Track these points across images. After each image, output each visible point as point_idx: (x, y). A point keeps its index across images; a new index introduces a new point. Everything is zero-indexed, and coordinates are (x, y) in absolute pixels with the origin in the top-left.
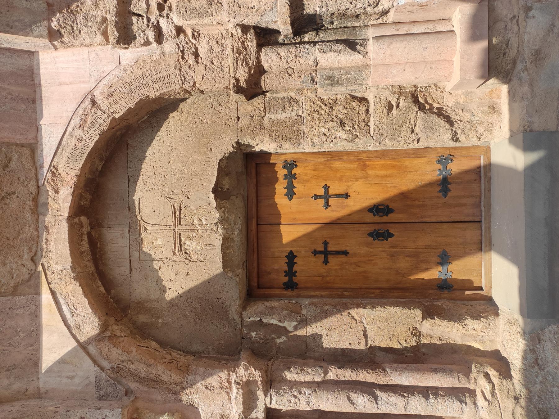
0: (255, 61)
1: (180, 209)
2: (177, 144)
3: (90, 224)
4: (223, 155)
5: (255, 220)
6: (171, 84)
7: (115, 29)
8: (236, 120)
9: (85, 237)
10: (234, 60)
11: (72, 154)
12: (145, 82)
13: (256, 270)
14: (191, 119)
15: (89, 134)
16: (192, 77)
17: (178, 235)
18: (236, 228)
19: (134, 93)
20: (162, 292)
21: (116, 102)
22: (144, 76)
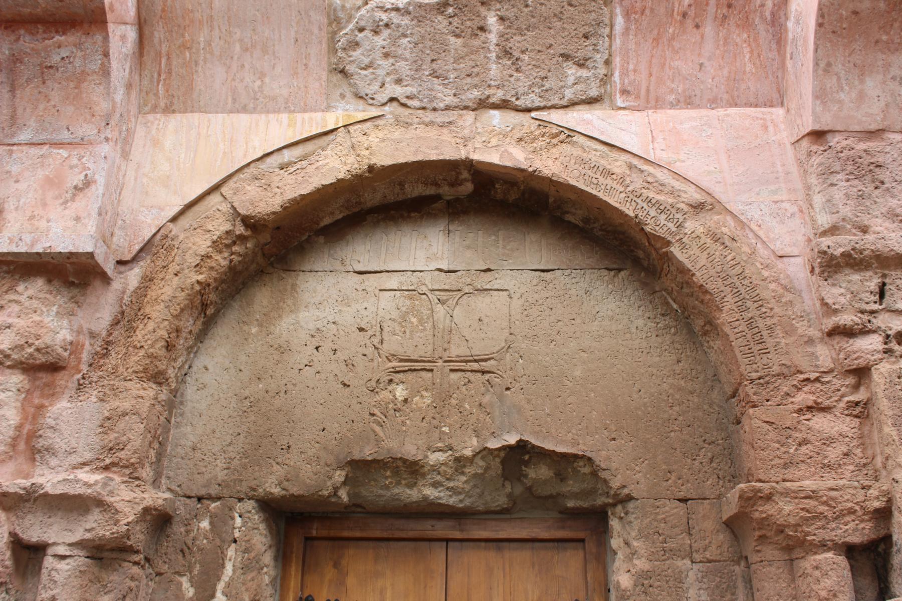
0: (814, 540)
1: (484, 372)
2: (622, 368)
3: (457, 200)
4: (603, 466)
5: (458, 535)
6: (749, 355)
7: (848, 248)
8: (681, 495)
9: (431, 191)
10: (813, 492)
11: (596, 168)
12: (749, 304)
13: (346, 534)
14: (677, 397)
15: (635, 199)
16: (768, 401)
17: (428, 366)
18: (439, 492)
19: (724, 282)
20: (312, 333)
21: (703, 248)
22: (760, 302)
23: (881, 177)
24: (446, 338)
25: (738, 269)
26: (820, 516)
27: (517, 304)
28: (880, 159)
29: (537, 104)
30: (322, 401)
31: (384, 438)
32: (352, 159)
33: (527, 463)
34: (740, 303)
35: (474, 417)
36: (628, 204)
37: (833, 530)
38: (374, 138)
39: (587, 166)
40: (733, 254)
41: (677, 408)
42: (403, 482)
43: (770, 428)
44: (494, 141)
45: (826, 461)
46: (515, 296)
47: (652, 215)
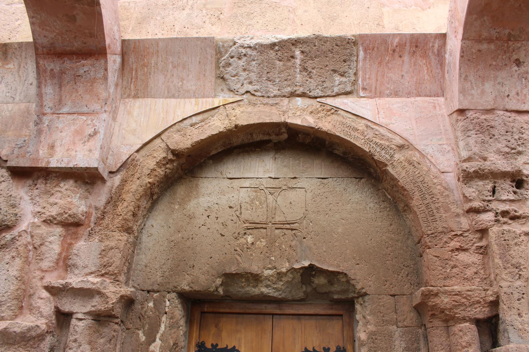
0: (459, 316)
1: (292, 230)
2: (362, 228)
3: (279, 142)
4: (352, 277)
5: (278, 312)
7: (477, 168)
8: (392, 293)
9: (266, 138)
10: (459, 292)
11: (349, 127)
12: (427, 196)
13: (222, 310)
14: (390, 243)
15: (369, 142)
16: (436, 245)
17: (264, 226)
18: (269, 290)
20: (206, 209)
21: (403, 168)
22: (432, 195)
23: (493, 133)
24: (273, 212)
25: (421, 179)
26: (462, 304)
27: (309, 195)
28: (493, 123)
29: (320, 94)
30: (210, 243)
32: (227, 122)
33: (314, 276)
34: (422, 196)
35: (287, 252)
36: (366, 145)
37: (469, 311)
38: (238, 111)
39: (345, 126)
40: (419, 171)
41: (390, 249)
42: (251, 285)
43: (437, 259)
44: (298, 113)
45: (466, 276)
46: (309, 191)
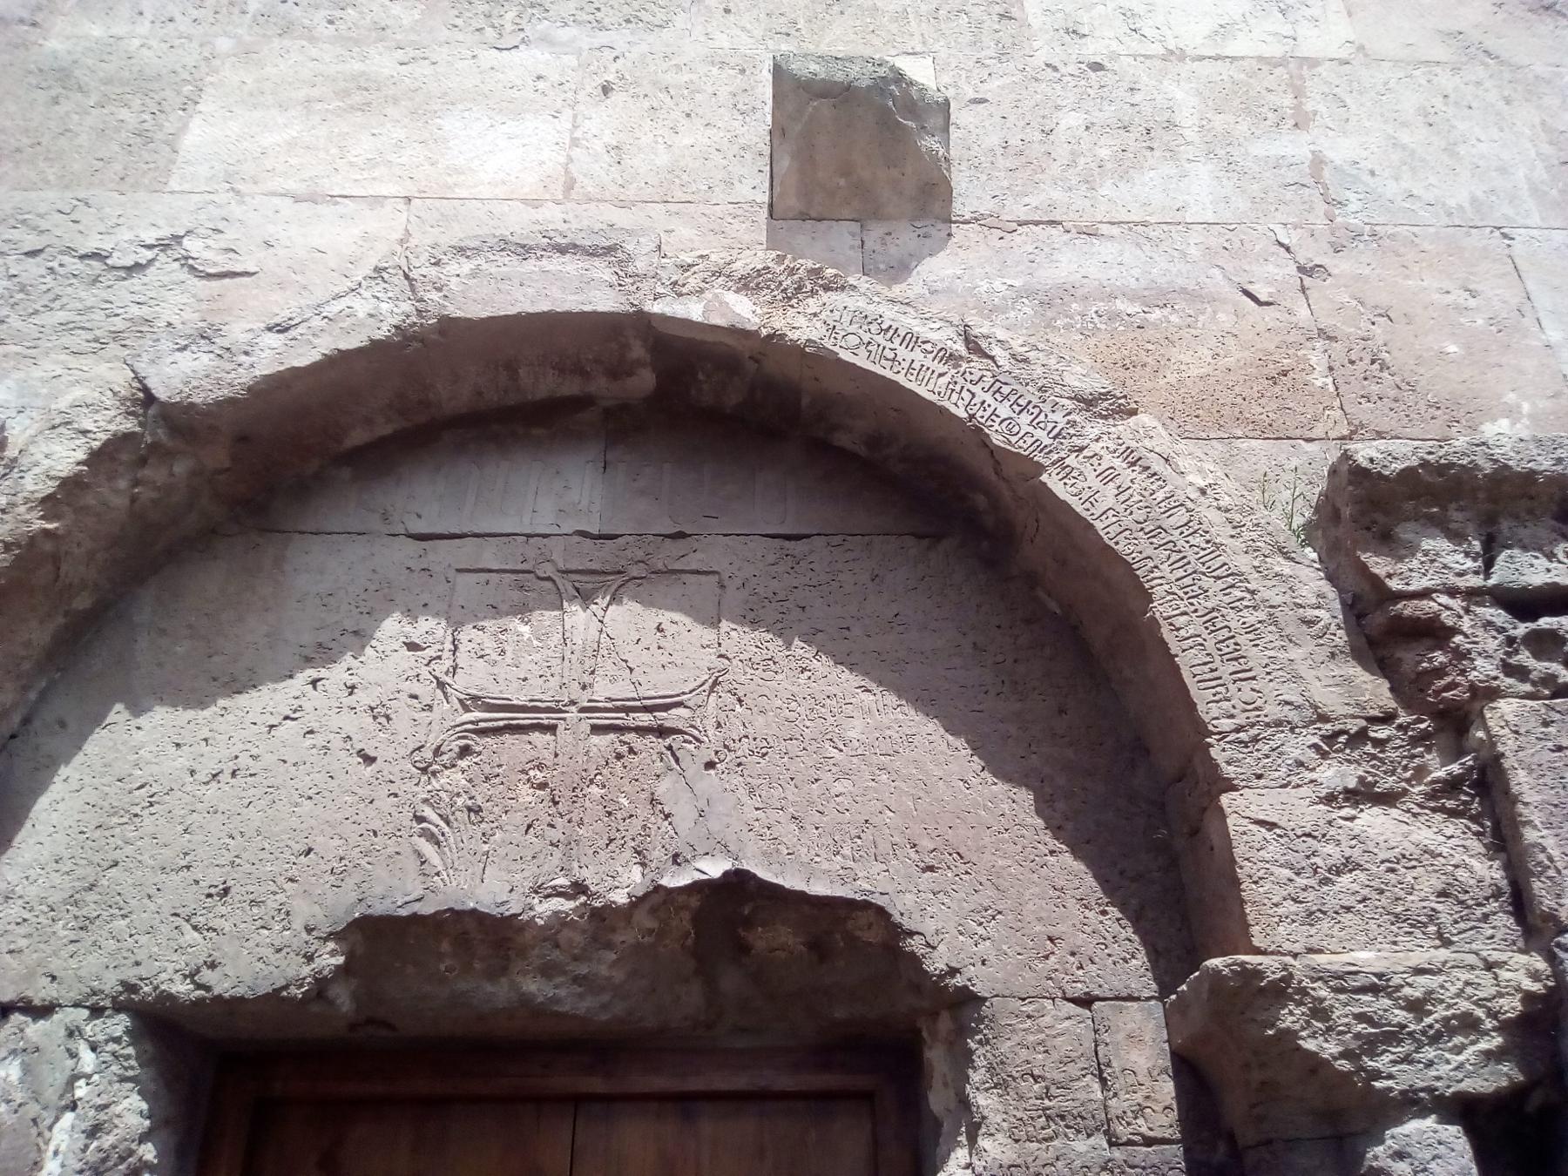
0: (1390, 1089)
1: (662, 732)
4: (907, 924)
6: (1214, 683)
7: (1414, 462)
8: (1079, 989)
9: (570, 387)
10: (1380, 976)
11: (892, 332)
16: (1259, 777)
17: (545, 719)
18: (556, 987)
19: (1154, 540)
20: (308, 652)
21: (1108, 476)
22: (1229, 579)
24: (589, 663)
25: (1181, 517)
26: (1394, 1036)
30: (310, 793)
31: (440, 868)
33: (748, 923)
34: (1187, 581)
35: (637, 823)
36: (955, 396)
39: (874, 328)
42: (477, 965)
43: (1268, 835)
45: (1399, 909)
46: (731, 586)
47: (1003, 416)
